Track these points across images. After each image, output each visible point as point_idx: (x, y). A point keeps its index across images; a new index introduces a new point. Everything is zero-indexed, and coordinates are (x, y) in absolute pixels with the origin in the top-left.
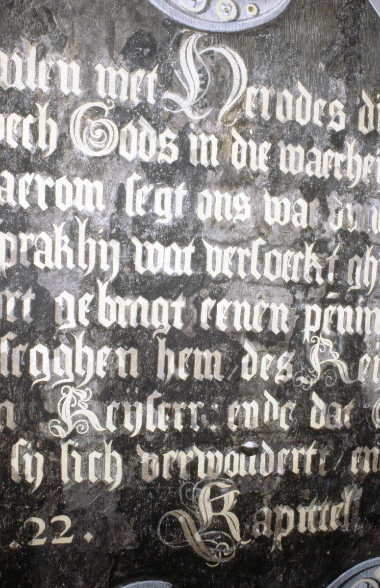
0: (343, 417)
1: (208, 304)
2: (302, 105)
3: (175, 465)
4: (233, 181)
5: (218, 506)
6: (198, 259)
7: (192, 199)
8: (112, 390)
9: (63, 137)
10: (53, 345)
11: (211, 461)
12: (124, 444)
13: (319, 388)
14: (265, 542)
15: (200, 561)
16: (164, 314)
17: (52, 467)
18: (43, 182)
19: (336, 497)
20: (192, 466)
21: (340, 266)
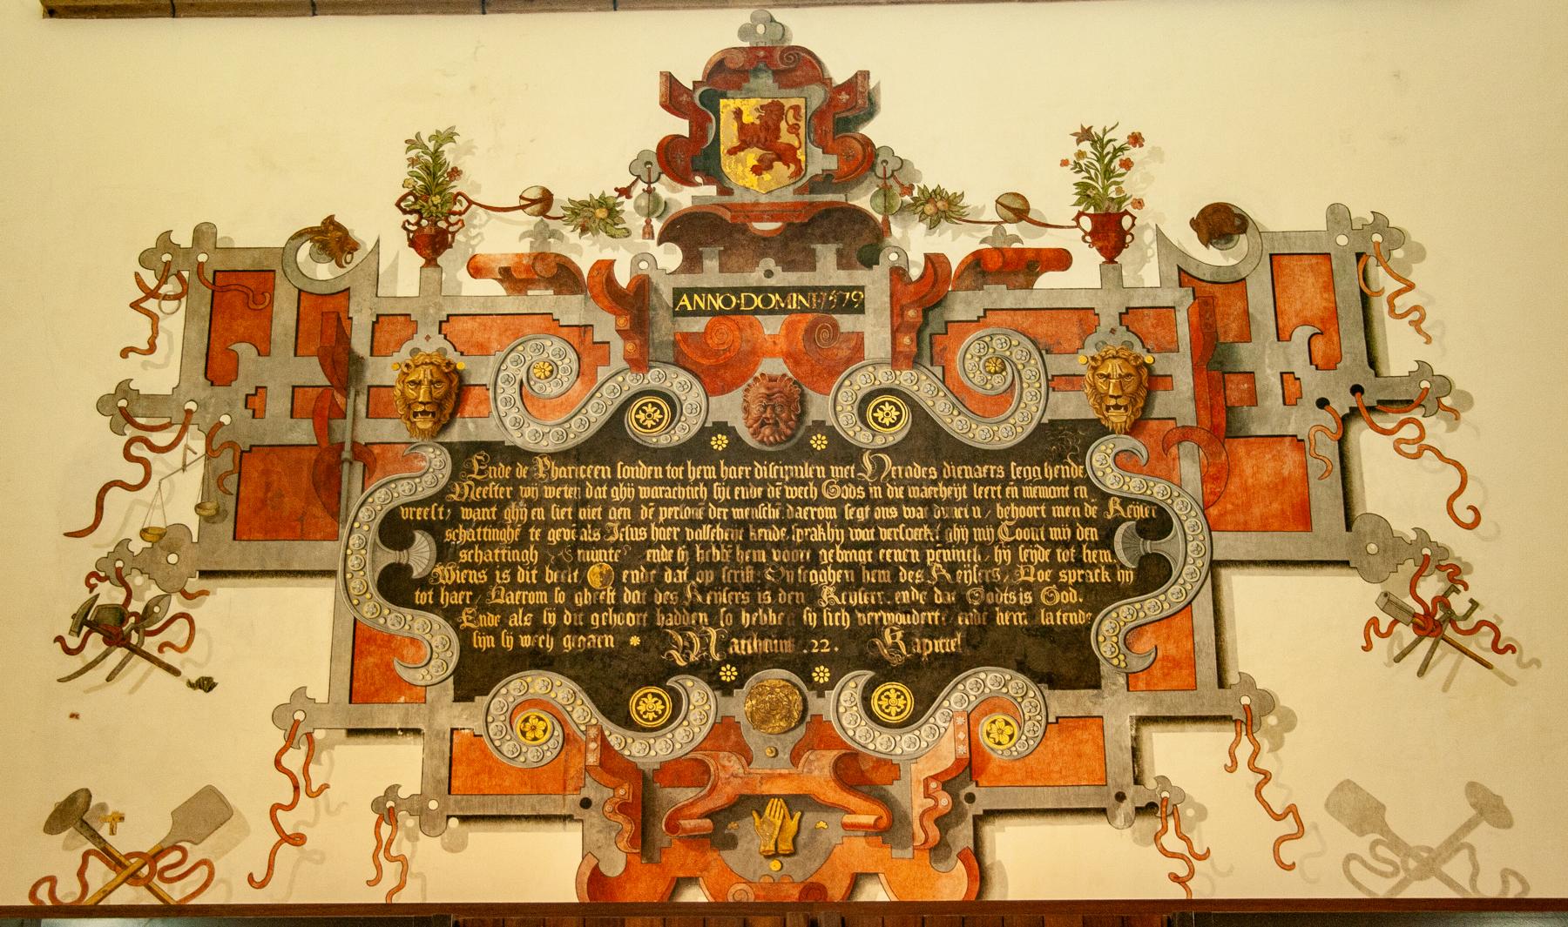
0: (951, 598)
1: (882, 551)
2: (917, 471)
3: (873, 619)
4: (887, 503)
5: (894, 637)
6: (877, 534)
7: (872, 512)
8: (842, 587)
9: (820, 494)
10: (818, 570)
11: (888, 617)
12: (850, 610)
13: (937, 585)
14: (919, 656)
15: (888, 663)
16: (863, 556)
17: (820, 619)
18: (812, 510)
19: (953, 636)
20: (881, 619)
21: (941, 533)
